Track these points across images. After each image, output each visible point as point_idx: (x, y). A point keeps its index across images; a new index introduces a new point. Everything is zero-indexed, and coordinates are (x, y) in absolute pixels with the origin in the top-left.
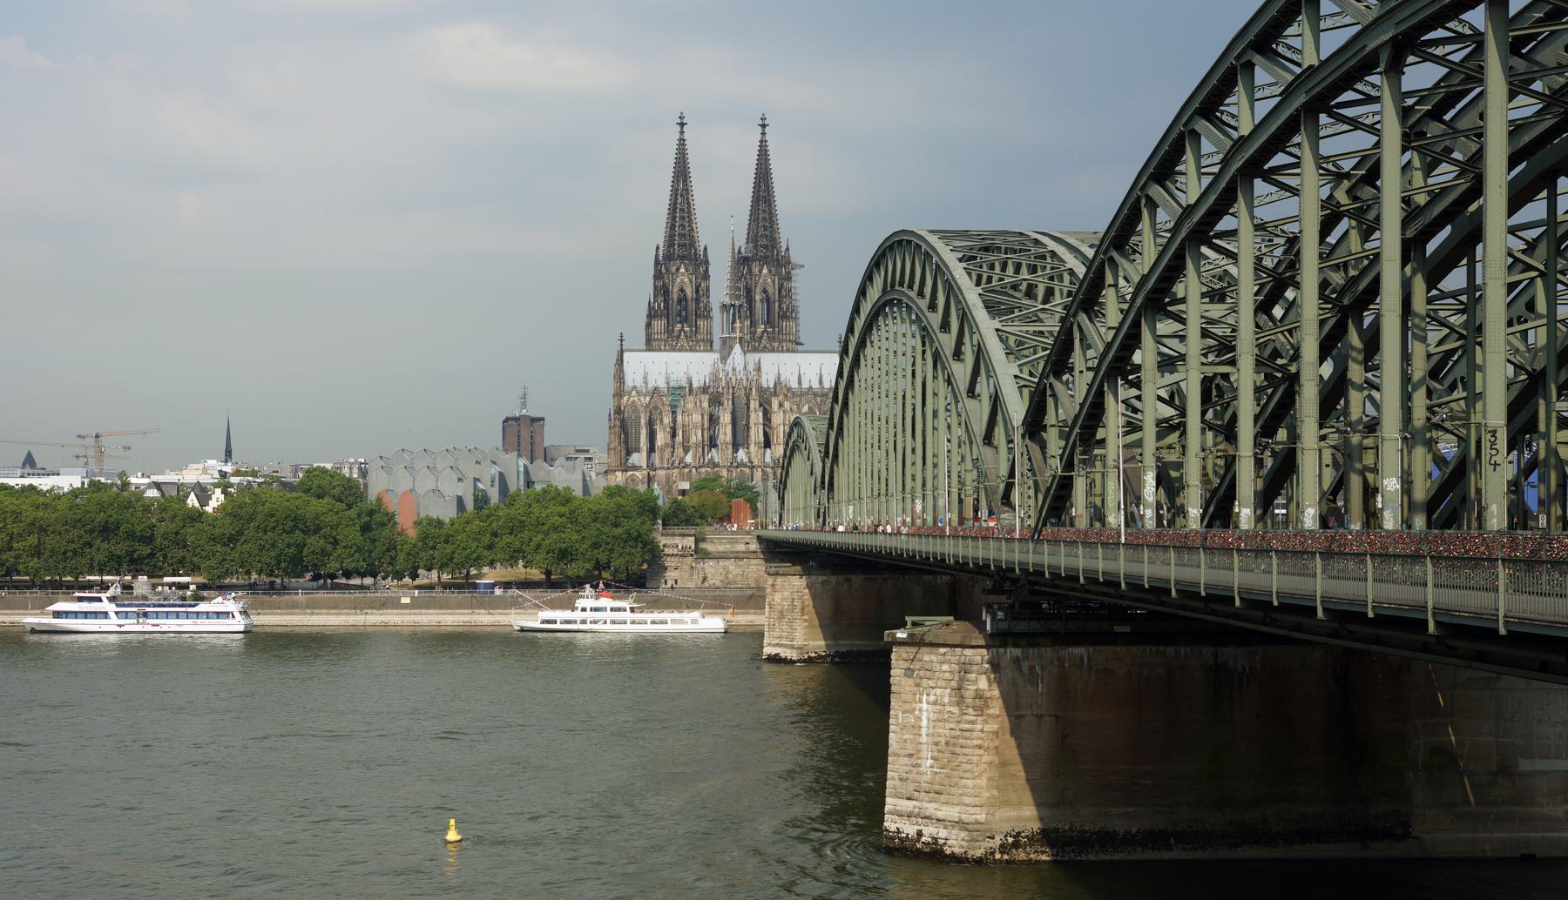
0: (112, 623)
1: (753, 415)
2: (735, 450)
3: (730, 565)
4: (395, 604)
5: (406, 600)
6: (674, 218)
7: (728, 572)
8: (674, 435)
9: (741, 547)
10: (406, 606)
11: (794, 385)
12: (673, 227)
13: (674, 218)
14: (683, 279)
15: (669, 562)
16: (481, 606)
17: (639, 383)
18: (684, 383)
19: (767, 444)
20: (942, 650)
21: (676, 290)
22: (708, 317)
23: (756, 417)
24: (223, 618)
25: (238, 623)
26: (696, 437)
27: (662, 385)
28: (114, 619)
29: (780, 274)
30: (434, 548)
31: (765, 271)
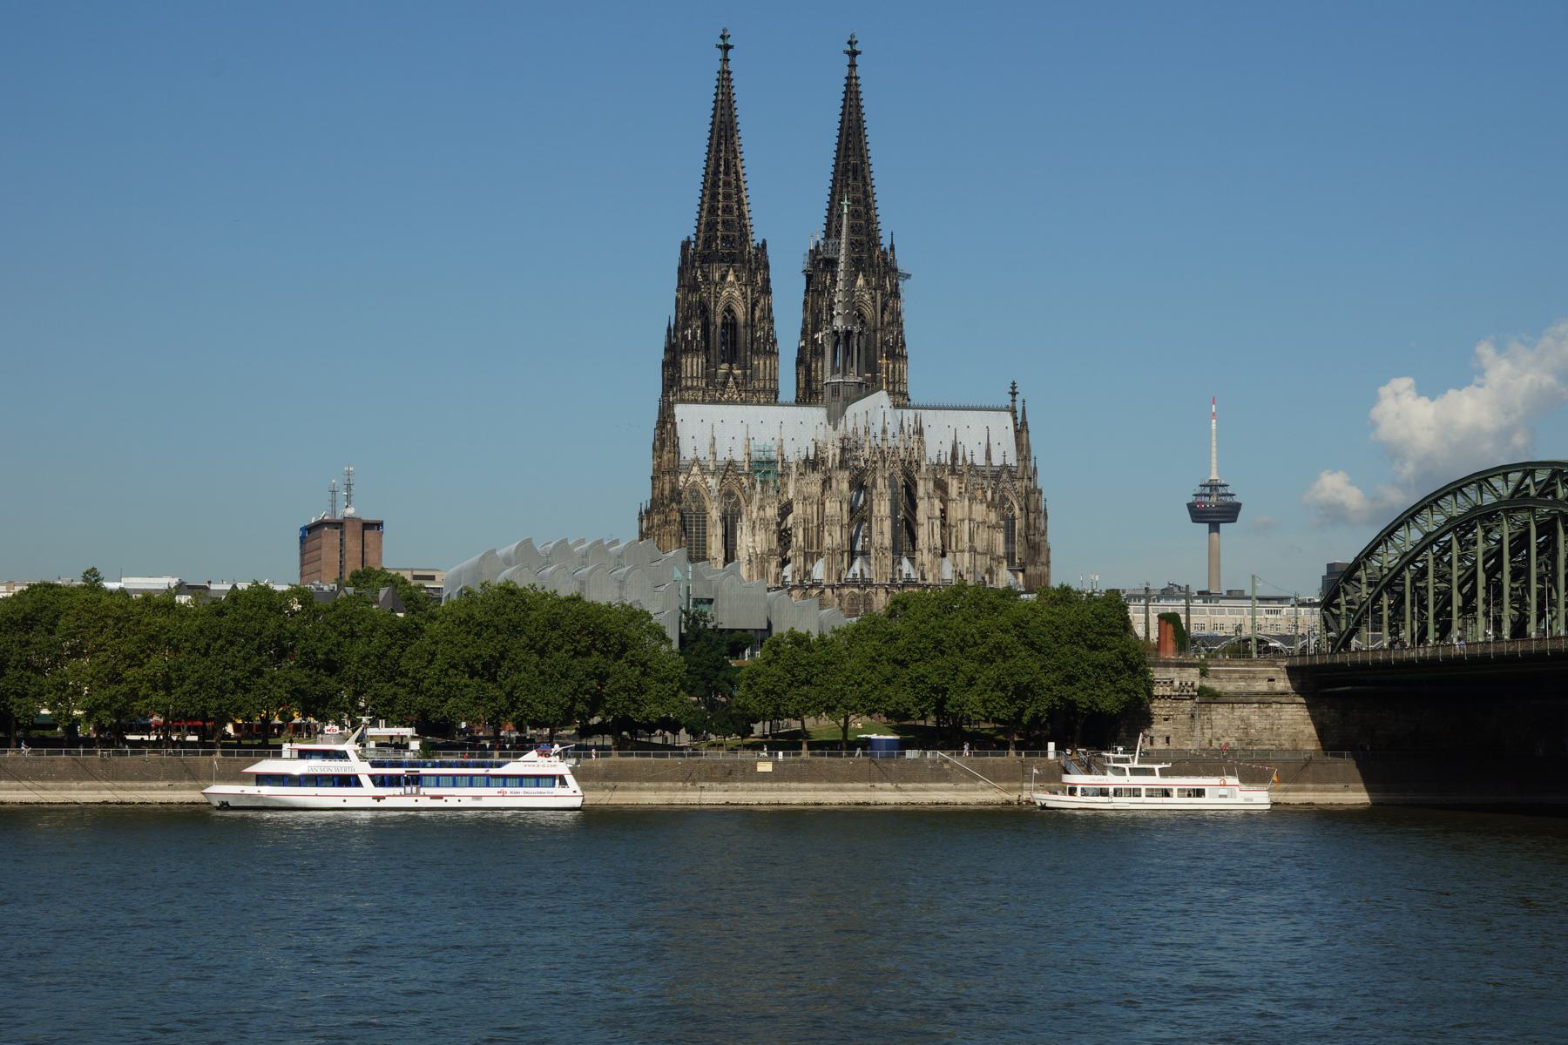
0: (363, 797)
1: (922, 506)
2: (897, 562)
3: (1250, 712)
4: (753, 776)
5: (765, 767)
6: (714, 196)
7: (1249, 725)
9: (1262, 686)
10: (764, 777)
12: (712, 210)
13: (714, 196)
14: (731, 292)
15: (1158, 708)
16: (885, 776)
17: (704, 453)
18: (774, 455)
21: (719, 309)
22: (773, 354)
24: (544, 783)
25: (570, 796)
26: (834, 538)
27: (739, 456)
28: (368, 787)
29: (883, 287)
30: (808, 682)
31: (860, 282)
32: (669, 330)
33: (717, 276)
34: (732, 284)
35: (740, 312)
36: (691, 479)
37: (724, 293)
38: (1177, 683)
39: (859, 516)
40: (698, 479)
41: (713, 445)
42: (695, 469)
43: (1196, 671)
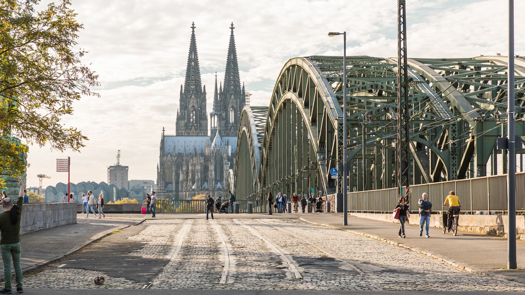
21: (190, 106)
22: (206, 119)
26: (198, 176)
27: (182, 151)
33: (189, 96)
34: (193, 99)
35: (196, 106)
37: (191, 101)
39: (206, 169)
41: (174, 148)
42: (169, 156)
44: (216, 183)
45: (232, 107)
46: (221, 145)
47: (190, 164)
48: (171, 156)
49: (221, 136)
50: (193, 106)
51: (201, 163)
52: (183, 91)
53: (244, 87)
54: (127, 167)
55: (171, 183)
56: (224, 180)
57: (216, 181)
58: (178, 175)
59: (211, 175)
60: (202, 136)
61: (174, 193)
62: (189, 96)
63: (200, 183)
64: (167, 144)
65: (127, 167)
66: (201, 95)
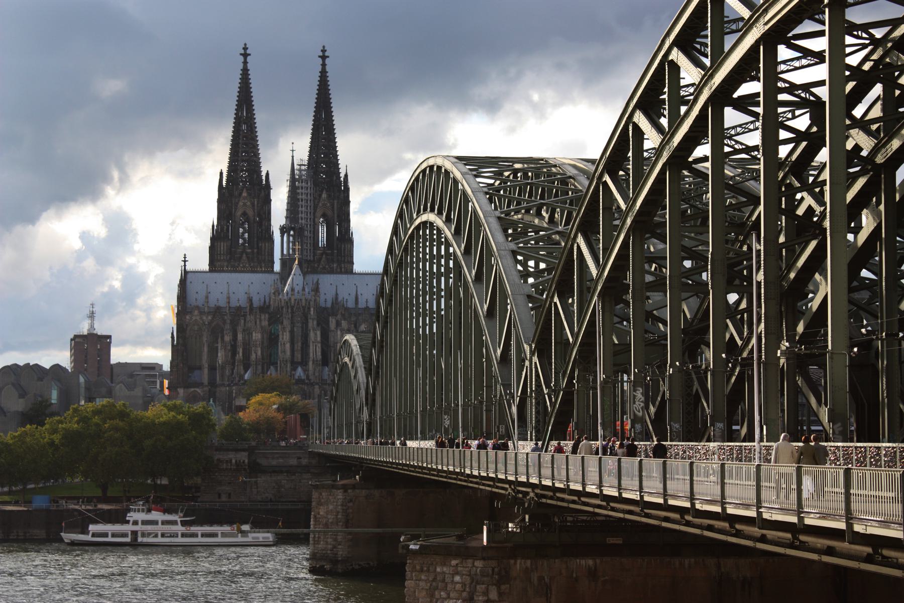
8: (234, 353)
9: (293, 462)
11: (351, 304)
19: (325, 361)
20: (454, 562)
21: (239, 213)
22: (271, 240)
23: (315, 336)
26: (256, 354)
27: (222, 303)
31: (324, 195)
32: (213, 226)
33: (236, 193)
34: (245, 198)
35: (250, 213)
36: (194, 318)
37: (241, 204)
38: (234, 461)
40: (198, 318)
41: (207, 297)
43: (246, 454)
44: (295, 369)
45: (324, 216)
46: (304, 289)
47: (240, 329)
48: (202, 313)
49: (305, 274)
50: (244, 214)
51: (262, 327)
52: (224, 183)
53: (346, 176)
54: (110, 337)
55: (200, 368)
56: (311, 363)
57: (294, 365)
58: (213, 352)
59: (284, 352)
60: (262, 272)
61: (206, 389)
62: (236, 193)
63: (260, 367)
64: (191, 288)
65: (110, 337)
66: (263, 191)
